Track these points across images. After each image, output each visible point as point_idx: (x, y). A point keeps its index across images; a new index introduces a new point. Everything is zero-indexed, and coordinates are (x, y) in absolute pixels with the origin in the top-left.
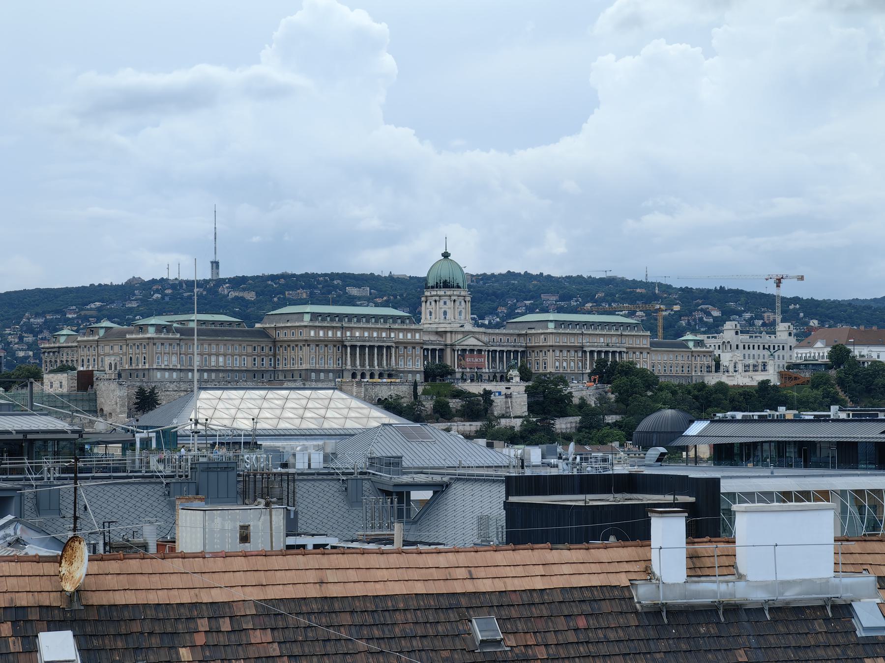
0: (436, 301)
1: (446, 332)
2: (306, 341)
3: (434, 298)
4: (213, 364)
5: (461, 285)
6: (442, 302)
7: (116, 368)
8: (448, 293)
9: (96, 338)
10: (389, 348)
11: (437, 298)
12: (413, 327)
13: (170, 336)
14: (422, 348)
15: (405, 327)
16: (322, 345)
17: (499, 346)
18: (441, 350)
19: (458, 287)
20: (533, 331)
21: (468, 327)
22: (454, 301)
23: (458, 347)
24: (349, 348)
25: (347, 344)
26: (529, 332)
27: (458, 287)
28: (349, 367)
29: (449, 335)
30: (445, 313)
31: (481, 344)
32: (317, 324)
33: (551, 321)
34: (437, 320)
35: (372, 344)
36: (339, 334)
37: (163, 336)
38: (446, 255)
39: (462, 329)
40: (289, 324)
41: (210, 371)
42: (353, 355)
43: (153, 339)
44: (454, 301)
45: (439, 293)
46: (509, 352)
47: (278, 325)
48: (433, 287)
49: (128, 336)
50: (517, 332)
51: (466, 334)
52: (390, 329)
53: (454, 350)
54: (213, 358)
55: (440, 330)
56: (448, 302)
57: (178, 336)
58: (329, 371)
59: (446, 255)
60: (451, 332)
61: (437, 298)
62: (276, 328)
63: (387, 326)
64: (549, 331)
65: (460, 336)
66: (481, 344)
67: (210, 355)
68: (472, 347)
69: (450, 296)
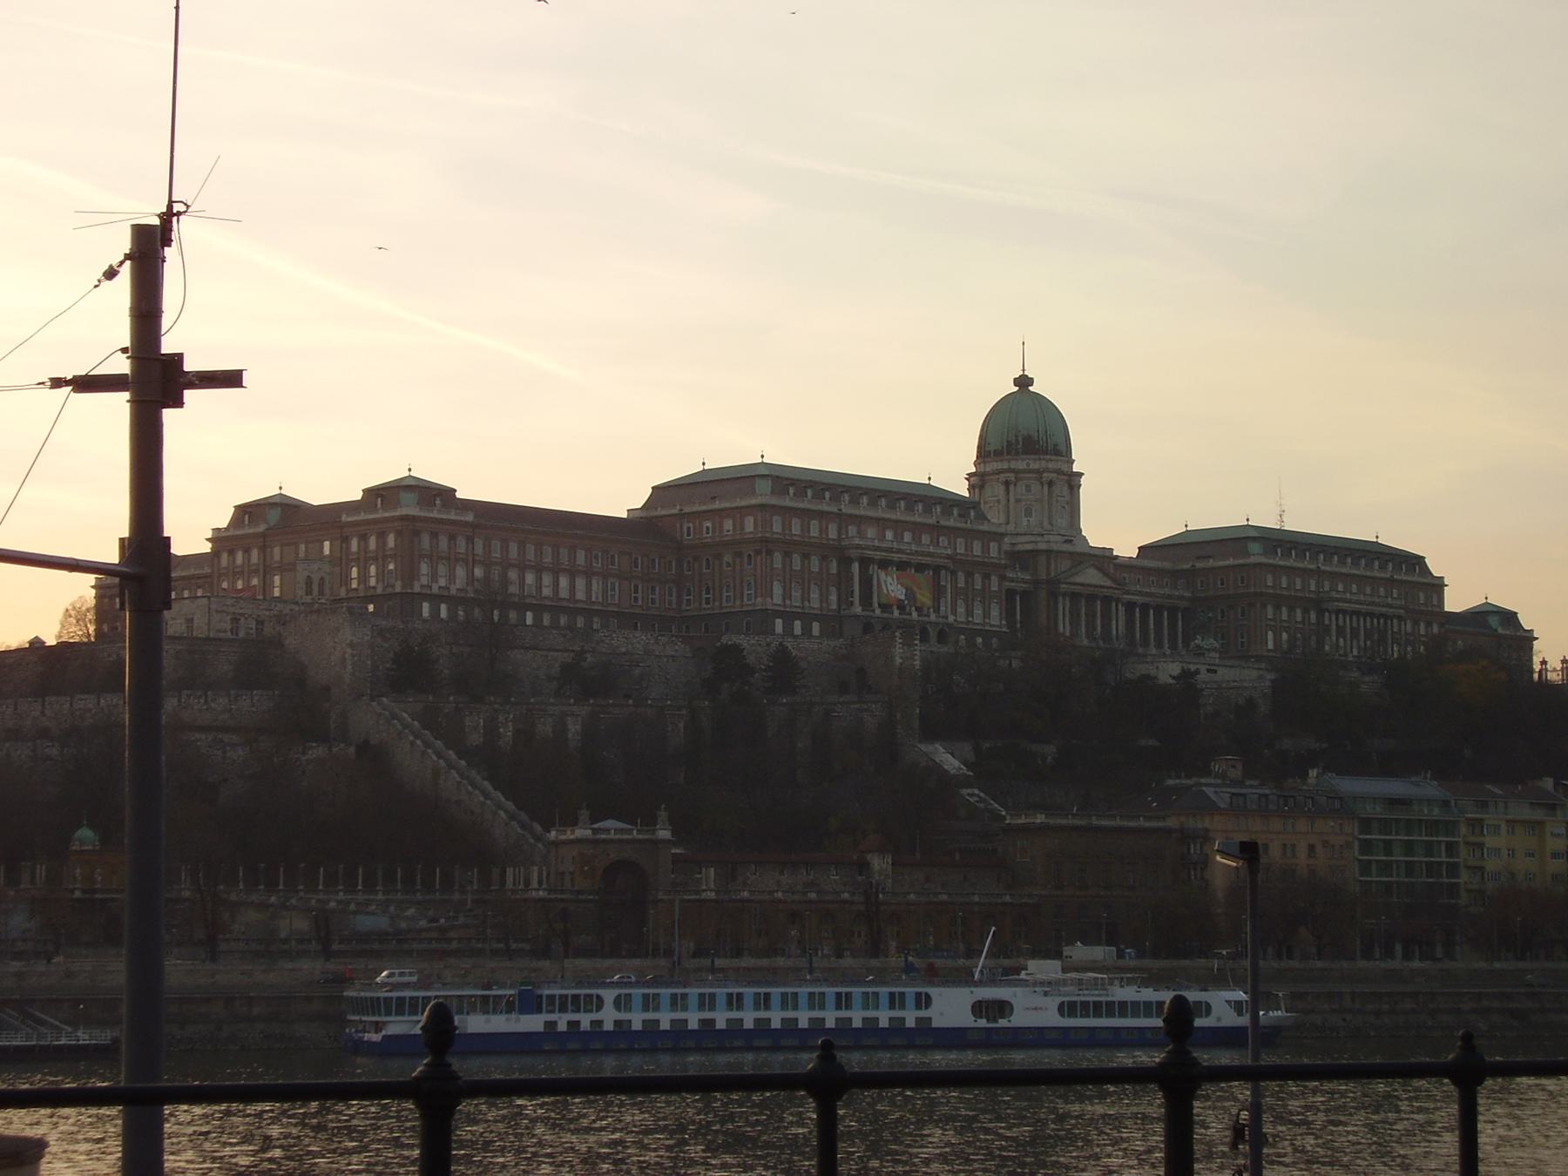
0: (1007, 484)
1: (1035, 553)
2: (764, 540)
3: (1002, 477)
5: (1062, 448)
6: (1021, 487)
7: (321, 593)
8: (1035, 465)
9: (262, 528)
11: (1012, 477)
13: (452, 516)
18: (1025, 595)
19: (1057, 452)
20: (1211, 563)
22: (1050, 484)
24: (856, 567)
25: (853, 553)
26: (1199, 565)
27: (1057, 452)
28: (858, 609)
29: (1043, 559)
30: (1028, 513)
31: (1109, 583)
32: (787, 502)
33: (1254, 539)
34: (1011, 528)
36: (833, 533)
37: (435, 514)
38: (1023, 382)
40: (717, 505)
41: (538, 609)
43: (413, 519)
44: (1050, 484)
45: (1013, 465)
46: (1159, 609)
47: (687, 509)
48: (998, 454)
49: (344, 518)
50: (1167, 565)
53: (1053, 595)
55: (1021, 548)
56: (1035, 487)
57: (470, 517)
58: (816, 617)
59: (1023, 382)
60: (1049, 552)
61: (1012, 477)
62: (681, 516)
63: (932, 521)
64: (1252, 560)
65: (1065, 564)
66: (1109, 583)
69: (1039, 472)
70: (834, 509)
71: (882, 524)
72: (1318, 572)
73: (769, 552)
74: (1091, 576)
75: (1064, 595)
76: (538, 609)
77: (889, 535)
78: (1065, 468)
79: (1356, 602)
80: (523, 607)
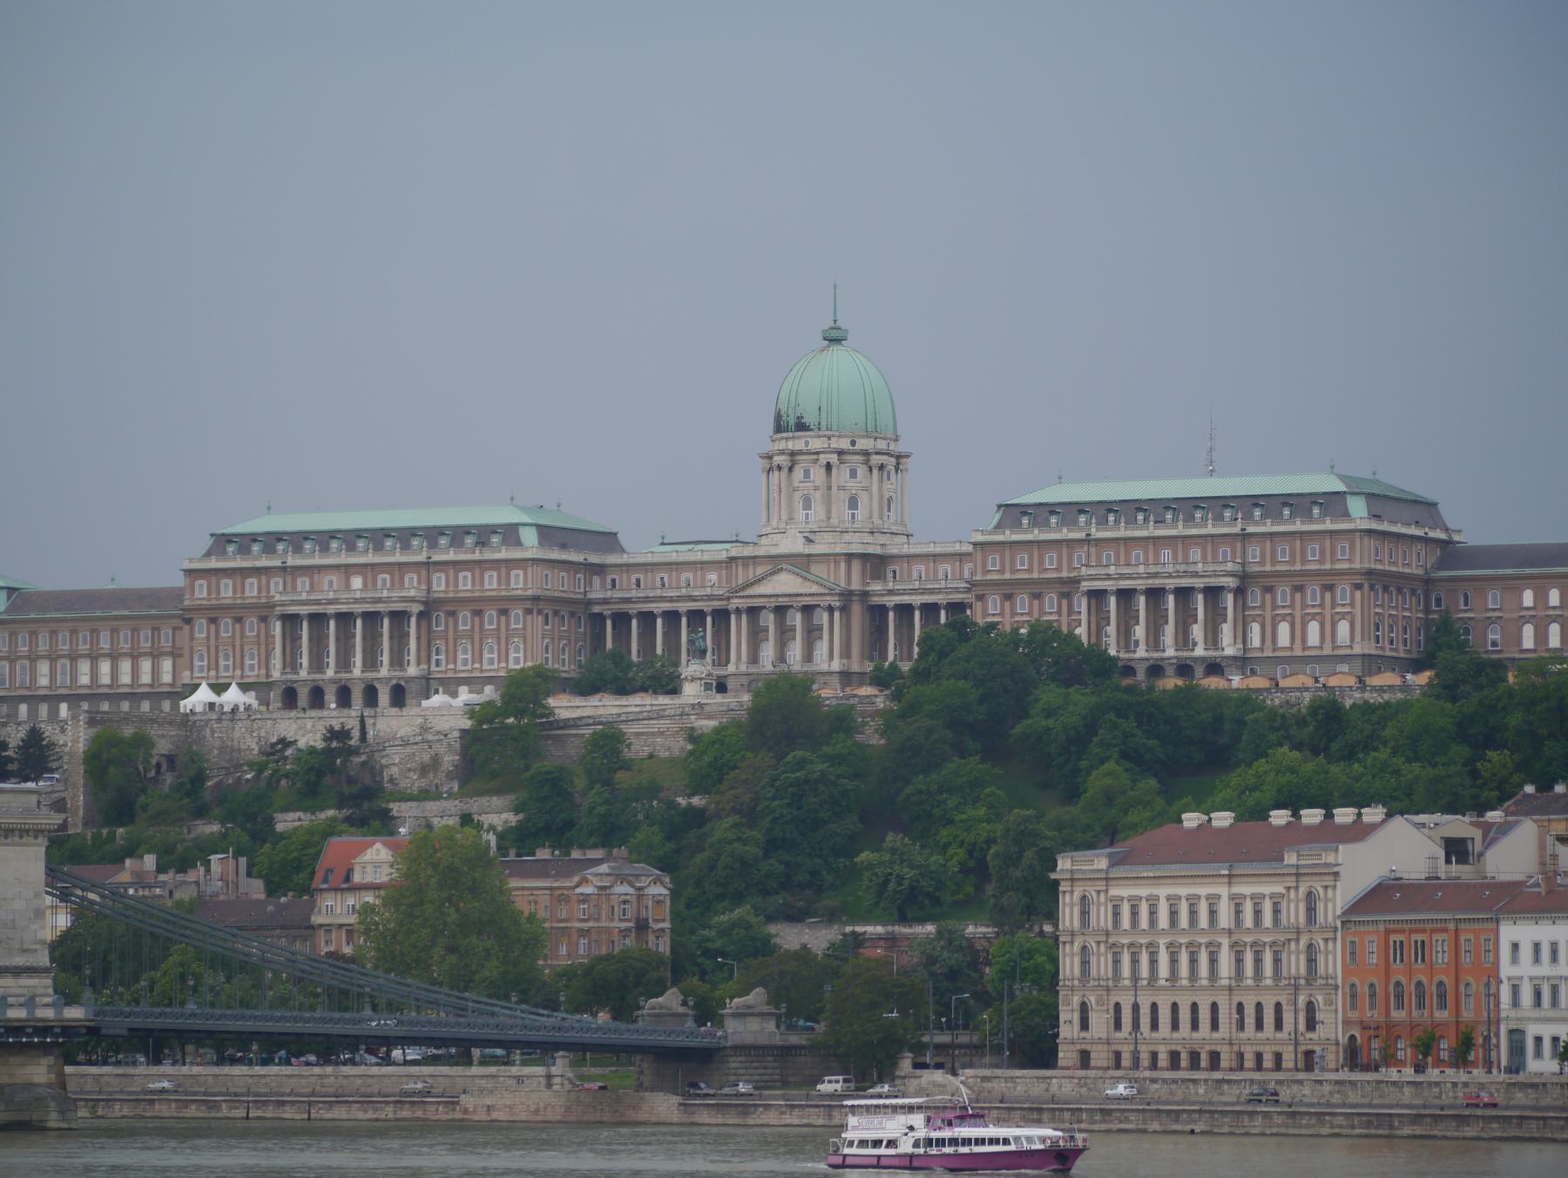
4: (85, 680)
10: (399, 617)
12: (503, 554)
14: (528, 611)
15: (477, 556)
16: (226, 621)
17: (914, 591)
19: (801, 427)
21: (792, 544)
23: (735, 603)
27: (801, 427)
32: (214, 563)
35: (344, 608)
39: (774, 551)
42: (291, 638)
51: (778, 562)
52: (429, 565)
54: (84, 667)
63: (421, 558)
65: (760, 570)
66: (815, 589)
67: (74, 658)
68: (783, 601)
70: (277, 563)
71: (348, 570)
72: (1088, 541)
73: (189, 621)
74: (785, 584)
75: (738, 611)
76: (74, 699)
77: (357, 582)
78: (816, 444)
79: (1122, 577)
80: (54, 700)
